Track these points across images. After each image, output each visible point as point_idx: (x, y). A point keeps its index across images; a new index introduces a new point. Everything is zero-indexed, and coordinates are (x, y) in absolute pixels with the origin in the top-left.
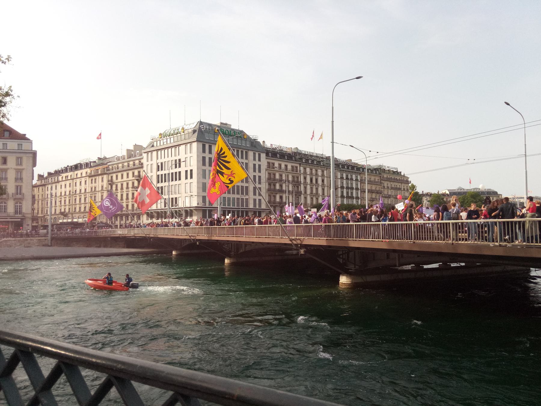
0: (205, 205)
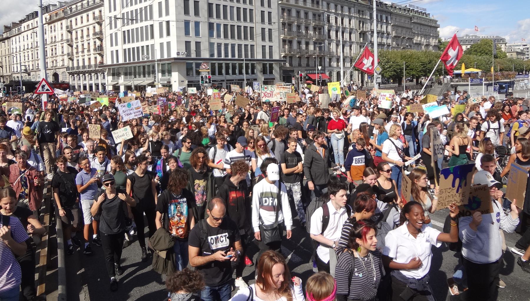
0: (190, 56)
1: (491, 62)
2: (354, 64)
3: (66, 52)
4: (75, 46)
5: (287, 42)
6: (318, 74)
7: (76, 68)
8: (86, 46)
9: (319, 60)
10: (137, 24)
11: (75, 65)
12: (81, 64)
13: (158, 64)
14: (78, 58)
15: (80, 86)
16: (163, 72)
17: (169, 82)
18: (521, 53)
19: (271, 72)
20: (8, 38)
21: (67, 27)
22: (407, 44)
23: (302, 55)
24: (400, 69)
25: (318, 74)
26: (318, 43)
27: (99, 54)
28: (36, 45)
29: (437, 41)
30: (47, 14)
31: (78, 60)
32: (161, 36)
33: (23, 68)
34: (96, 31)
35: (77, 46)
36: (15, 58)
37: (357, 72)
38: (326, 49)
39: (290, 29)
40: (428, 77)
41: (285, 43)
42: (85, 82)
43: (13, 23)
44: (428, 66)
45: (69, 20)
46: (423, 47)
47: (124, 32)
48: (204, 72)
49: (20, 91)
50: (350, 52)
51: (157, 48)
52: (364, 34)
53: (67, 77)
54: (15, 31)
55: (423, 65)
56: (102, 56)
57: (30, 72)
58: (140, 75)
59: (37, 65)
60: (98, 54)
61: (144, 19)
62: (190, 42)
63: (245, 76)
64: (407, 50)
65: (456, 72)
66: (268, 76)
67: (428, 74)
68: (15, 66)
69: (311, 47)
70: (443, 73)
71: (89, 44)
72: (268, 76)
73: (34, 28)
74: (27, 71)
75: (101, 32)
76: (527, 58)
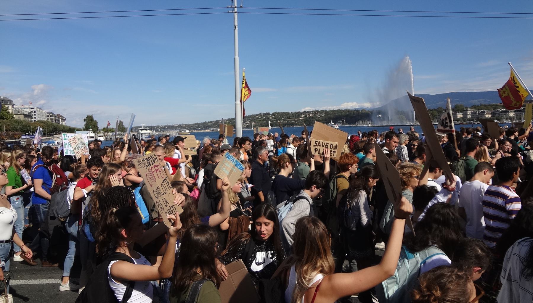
18: (29, 116)
76: (34, 120)
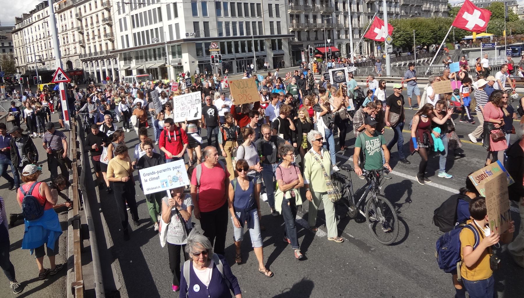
0: (199, 36)
1: (503, 26)
2: (363, 35)
3: (77, 40)
4: (85, 34)
5: (295, 16)
6: (327, 47)
7: (88, 55)
8: (96, 33)
9: (327, 32)
10: (145, 8)
11: (88, 52)
12: (93, 51)
13: (168, 46)
14: (89, 45)
15: (93, 73)
16: (174, 54)
17: (180, 64)
19: (280, 48)
20: (20, 29)
21: (77, 15)
22: (416, 12)
23: (310, 29)
24: (410, 38)
25: (327, 47)
26: (325, 16)
27: (110, 40)
28: (48, 35)
29: (446, 7)
30: (56, 3)
31: (90, 47)
32: (169, 18)
33: (38, 58)
34: (105, 17)
35: (88, 33)
36: (29, 49)
37: (366, 43)
38: (334, 22)
39: (297, 3)
40: (440, 44)
41: (293, 18)
42: (98, 68)
43: (24, 14)
44: (438, 33)
45: (78, 8)
46: (432, 14)
47: (133, 16)
48: (214, 51)
49: (36, 80)
50: (359, 23)
51: (166, 30)
52: (371, 4)
53: (81, 64)
54: (26, 22)
55: (434, 32)
56: (113, 41)
57: (44, 62)
58: (151, 58)
59: (50, 55)
60: (108, 39)
61: (151, 2)
62: (198, 22)
63: (254, 54)
64: (416, 18)
65: (467, 37)
66: (277, 52)
67: (439, 42)
68: (30, 56)
69: (319, 21)
70: (454, 39)
71: (99, 30)
72: (277, 52)
73: (44, 18)
74: (41, 61)
75: (110, 18)
